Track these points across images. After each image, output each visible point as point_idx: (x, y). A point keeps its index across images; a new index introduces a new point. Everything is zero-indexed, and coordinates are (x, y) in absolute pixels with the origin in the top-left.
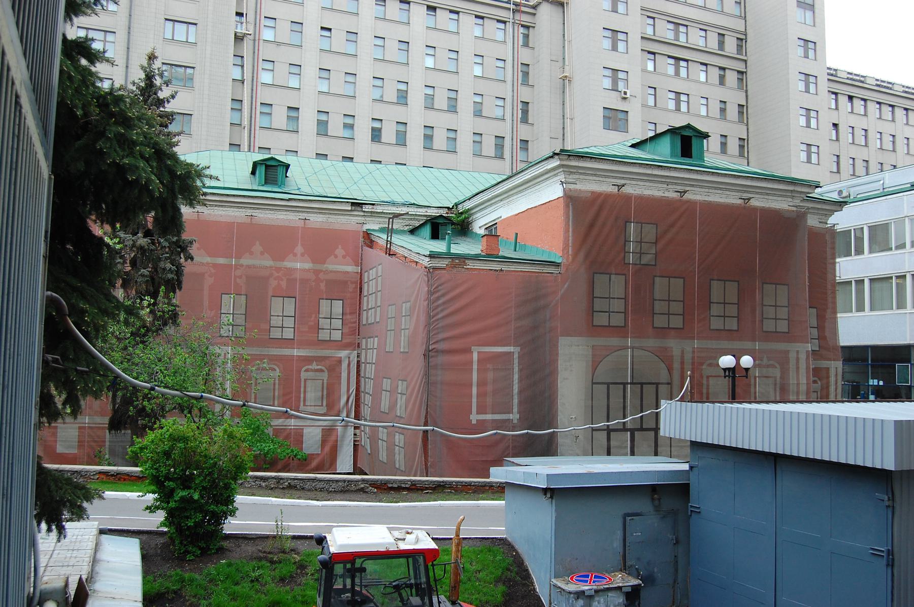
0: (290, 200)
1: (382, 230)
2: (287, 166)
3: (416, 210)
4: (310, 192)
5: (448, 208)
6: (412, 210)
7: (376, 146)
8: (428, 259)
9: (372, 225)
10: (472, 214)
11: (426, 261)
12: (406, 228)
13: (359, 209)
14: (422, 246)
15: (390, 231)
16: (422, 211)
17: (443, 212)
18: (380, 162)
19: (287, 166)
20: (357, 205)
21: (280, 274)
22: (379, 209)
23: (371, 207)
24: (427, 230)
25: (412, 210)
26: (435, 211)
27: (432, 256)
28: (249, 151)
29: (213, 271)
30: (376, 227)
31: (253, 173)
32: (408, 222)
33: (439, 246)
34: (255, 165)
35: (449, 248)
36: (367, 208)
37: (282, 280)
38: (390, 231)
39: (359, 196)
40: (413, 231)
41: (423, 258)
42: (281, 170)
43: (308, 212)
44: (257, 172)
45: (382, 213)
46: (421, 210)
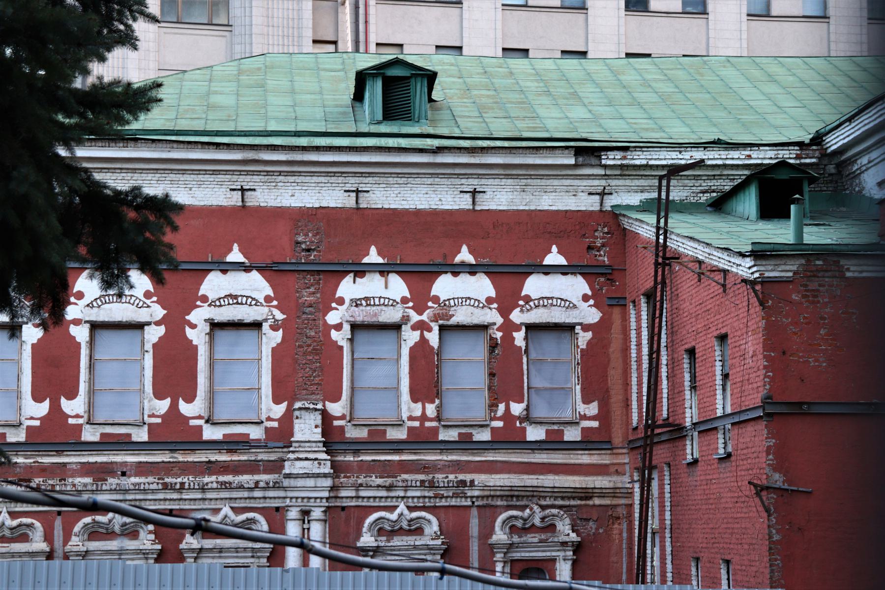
0: (439, 150)
1: (644, 207)
2: (431, 77)
3: (724, 154)
4: (457, 133)
5: (800, 144)
6: (714, 157)
7: (637, 20)
8: (749, 262)
9: (627, 196)
10: (852, 160)
11: (745, 268)
12: (704, 198)
13: (594, 161)
14: (747, 227)
15: (662, 207)
16: (736, 157)
17: (789, 155)
18: (649, 55)
19: (431, 77)
20: (588, 152)
21: (424, 317)
22: (639, 158)
23: (619, 155)
24: (749, 203)
25: (714, 157)
26: (771, 153)
27: (760, 253)
28: (357, 50)
29: (280, 316)
30: (635, 199)
31: (359, 96)
32: (706, 184)
33: (781, 233)
34: (362, 78)
35: (799, 234)
36: (612, 159)
37: (430, 330)
38: (662, 207)
39: (596, 133)
40: (720, 204)
41: (738, 260)
42: (419, 88)
43: (479, 176)
44: (367, 95)
45: (647, 167)
46: (735, 154)
